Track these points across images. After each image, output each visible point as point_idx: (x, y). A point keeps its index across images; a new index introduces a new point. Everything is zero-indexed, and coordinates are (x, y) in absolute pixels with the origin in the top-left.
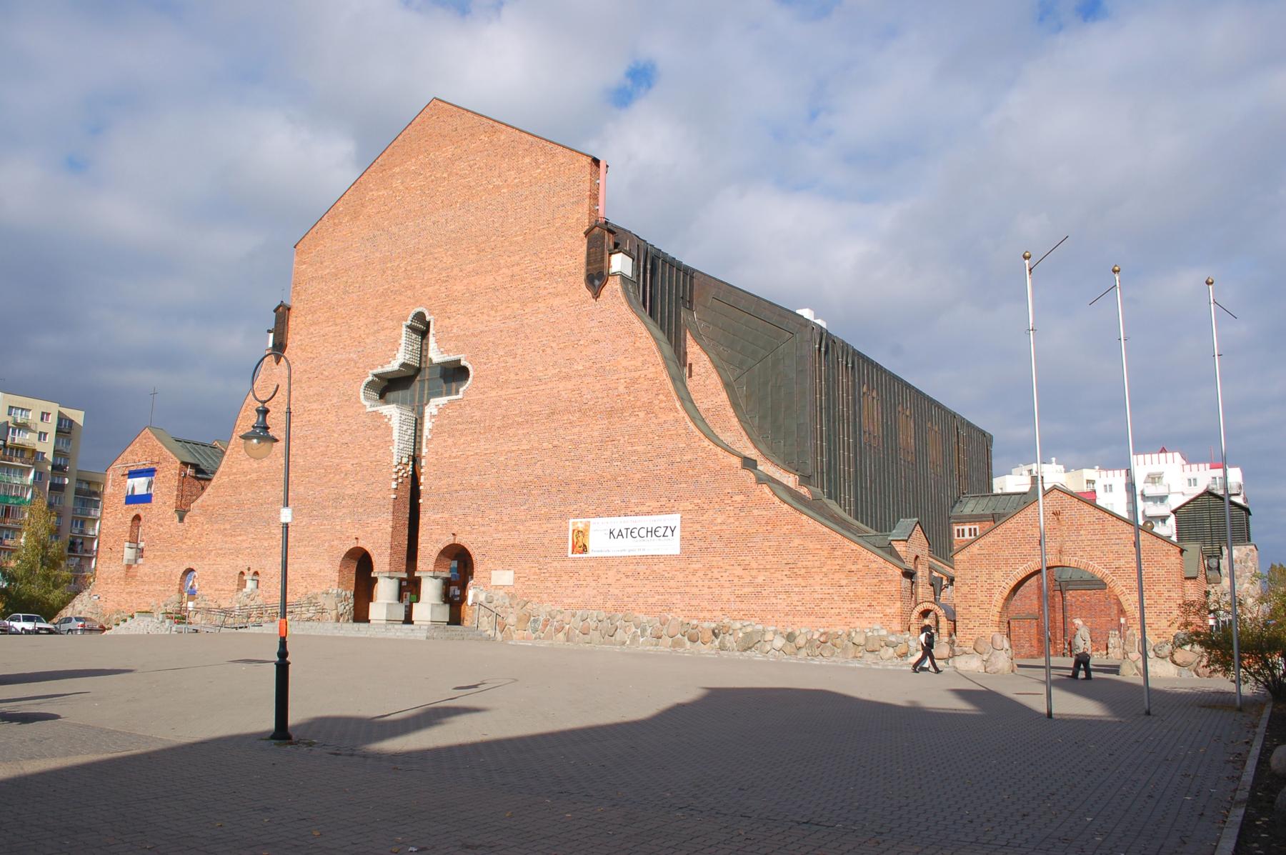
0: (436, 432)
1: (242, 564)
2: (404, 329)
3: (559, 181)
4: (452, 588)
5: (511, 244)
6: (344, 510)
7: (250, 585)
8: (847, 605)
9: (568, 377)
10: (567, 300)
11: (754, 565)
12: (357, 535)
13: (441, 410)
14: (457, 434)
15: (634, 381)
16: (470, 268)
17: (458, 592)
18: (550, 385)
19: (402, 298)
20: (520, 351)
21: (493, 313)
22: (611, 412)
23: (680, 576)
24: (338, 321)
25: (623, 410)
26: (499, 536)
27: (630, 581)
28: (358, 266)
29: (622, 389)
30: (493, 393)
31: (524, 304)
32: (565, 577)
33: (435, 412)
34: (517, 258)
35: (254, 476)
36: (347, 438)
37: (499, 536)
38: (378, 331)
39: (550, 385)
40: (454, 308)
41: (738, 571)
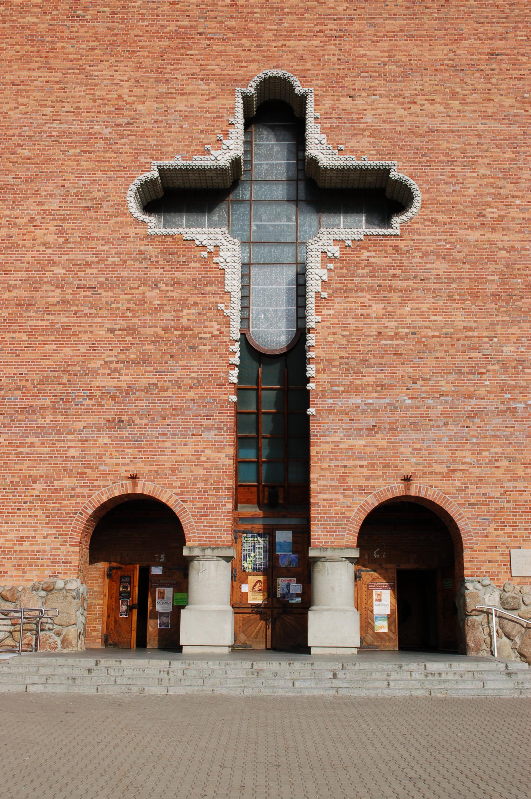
0: (342, 285)
4: (282, 582)
6: (92, 419)
12: (132, 469)
16: (392, 25)
17: (296, 588)
19: (230, 48)
21: (455, 104)
24: (57, 63)
30: (473, 236)
33: (335, 251)
36: (92, 277)
37: (520, 485)
38: (169, 95)
40: (359, 83)
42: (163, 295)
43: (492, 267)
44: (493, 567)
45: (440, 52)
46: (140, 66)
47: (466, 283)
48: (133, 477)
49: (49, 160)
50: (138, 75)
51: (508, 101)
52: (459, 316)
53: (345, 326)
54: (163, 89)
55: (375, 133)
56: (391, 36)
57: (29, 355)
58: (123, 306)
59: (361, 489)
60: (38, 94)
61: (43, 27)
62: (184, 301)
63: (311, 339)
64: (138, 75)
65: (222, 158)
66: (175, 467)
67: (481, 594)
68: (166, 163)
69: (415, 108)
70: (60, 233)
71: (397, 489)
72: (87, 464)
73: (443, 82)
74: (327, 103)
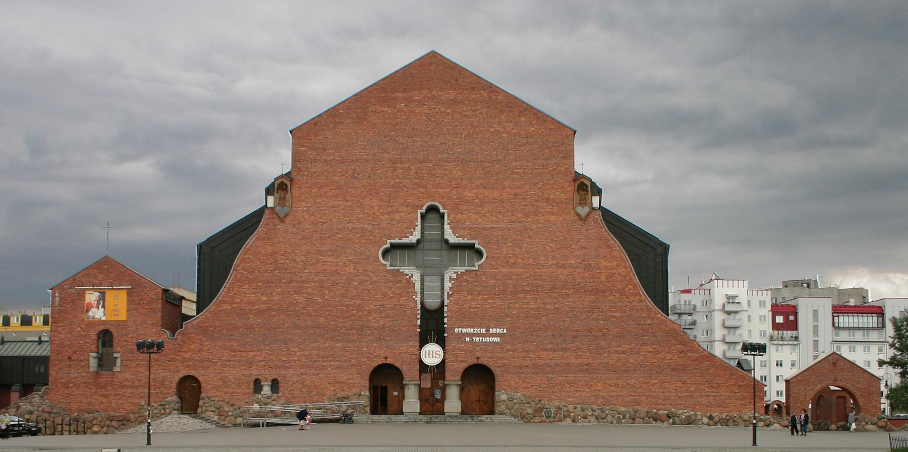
1: (255, 372)
2: (419, 215)
3: (550, 139)
5: (513, 173)
6: (370, 337)
7: (266, 390)
8: (739, 402)
9: (563, 267)
10: (561, 219)
11: (689, 381)
12: (385, 355)
13: (460, 276)
14: (475, 293)
15: (612, 275)
16: (478, 182)
18: (551, 270)
19: (415, 192)
20: (525, 245)
22: (597, 292)
23: (645, 386)
24: (349, 198)
25: (604, 292)
26: (516, 360)
27: (613, 388)
28: (367, 161)
29: (603, 278)
30: (505, 270)
31: (526, 216)
32: (567, 386)
33: (454, 276)
34: (519, 184)
35: (264, 306)
37: (516, 360)
38: (393, 212)
39: (551, 270)
40: (465, 207)
41: (680, 384)
42: (393, 293)
43: (510, 282)
44: (505, 387)
45: (496, 194)
46: (381, 200)
47: (501, 288)
48: (386, 358)
49: (349, 239)
50: (380, 204)
51: (520, 215)
52: (498, 300)
53: (458, 304)
54: (390, 209)
55: (470, 228)
56: (477, 187)
57: (347, 314)
58: (379, 297)
59: (462, 362)
60: (343, 212)
61: (342, 182)
62: (401, 295)
63: (446, 309)
64: (380, 204)
65: (413, 239)
66: (400, 354)
67: (501, 396)
68: (393, 241)
69: (485, 218)
70: (355, 269)
71: (475, 361)
72: (369, 353)
73: (496, 207)
74: (452, 216)
